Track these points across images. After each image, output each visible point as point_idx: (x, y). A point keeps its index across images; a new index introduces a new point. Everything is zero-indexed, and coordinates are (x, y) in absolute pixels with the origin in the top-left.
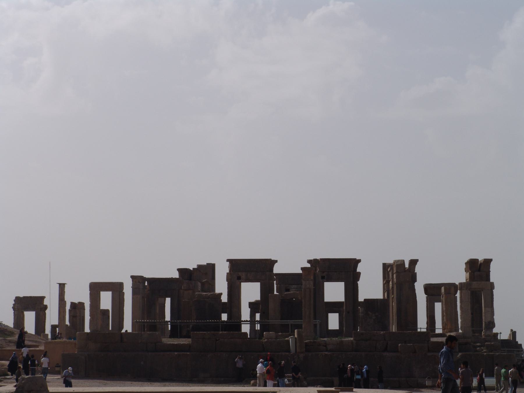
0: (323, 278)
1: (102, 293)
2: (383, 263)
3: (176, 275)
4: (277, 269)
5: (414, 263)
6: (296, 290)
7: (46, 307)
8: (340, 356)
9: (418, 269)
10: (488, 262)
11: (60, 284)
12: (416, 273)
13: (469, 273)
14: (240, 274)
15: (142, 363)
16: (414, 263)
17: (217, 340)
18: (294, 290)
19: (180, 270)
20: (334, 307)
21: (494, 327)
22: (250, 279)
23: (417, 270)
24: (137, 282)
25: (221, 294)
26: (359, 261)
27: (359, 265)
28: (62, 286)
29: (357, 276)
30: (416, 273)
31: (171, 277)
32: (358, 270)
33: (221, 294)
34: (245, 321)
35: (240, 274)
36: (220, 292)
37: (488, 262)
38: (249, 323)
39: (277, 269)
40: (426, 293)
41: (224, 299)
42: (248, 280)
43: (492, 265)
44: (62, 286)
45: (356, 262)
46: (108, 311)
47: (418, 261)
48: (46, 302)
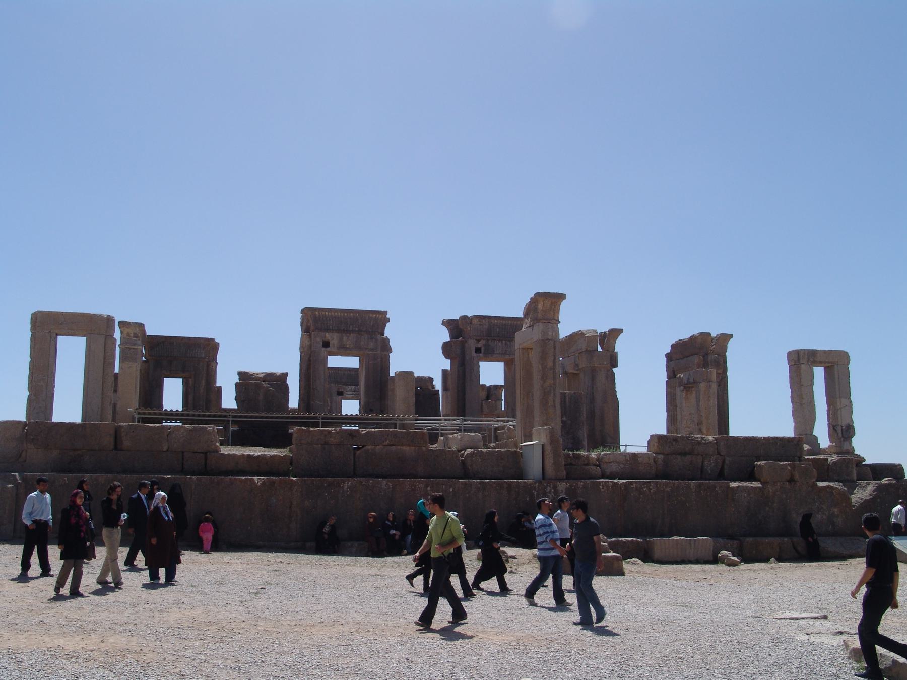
1: (63, 342)
2: (443, 370)
8: (645, 489)
12: (617, 352)
14: (328, 336)
18: (351, 393)
22: (348, 346)
24: (132, 335)
25: (285, 375)
30: (617, 352)
33: (285, 375)
35: (328, 336)
36: (284, 371)
37: (725, 338)
43: (731, 345)
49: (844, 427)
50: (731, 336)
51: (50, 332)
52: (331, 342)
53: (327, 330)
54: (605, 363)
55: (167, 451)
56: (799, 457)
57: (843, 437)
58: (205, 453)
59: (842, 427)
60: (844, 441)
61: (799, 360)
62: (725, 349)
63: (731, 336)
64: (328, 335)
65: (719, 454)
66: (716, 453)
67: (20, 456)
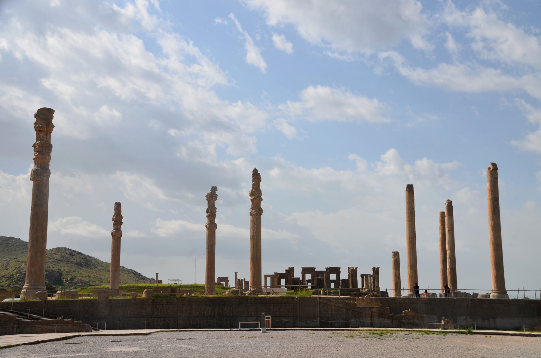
0: (330, 273)
3: (285, 272)
4: (316, 270)
5: (356, 268)
7: (228, 281)
9: (358, 270)
10: (378, 268)
11: (236, 273)
16: (356, 268)
19: (286, 270)
20: (333, 281)
25: (299, 278)
26: (340, 268)
27: (340, 269)
28: (236, 273)
29: (340, 272)
32: (340, 271)
33: (299, 278)
39: (316, 270)
40: (361, 277)
41: (301, 279)
42: (308, 274)
44: (236, 273)
45: (339, 268)
46: (248, 282)
48: (229, 279)
50: (379, 268)
53: (305, 271)
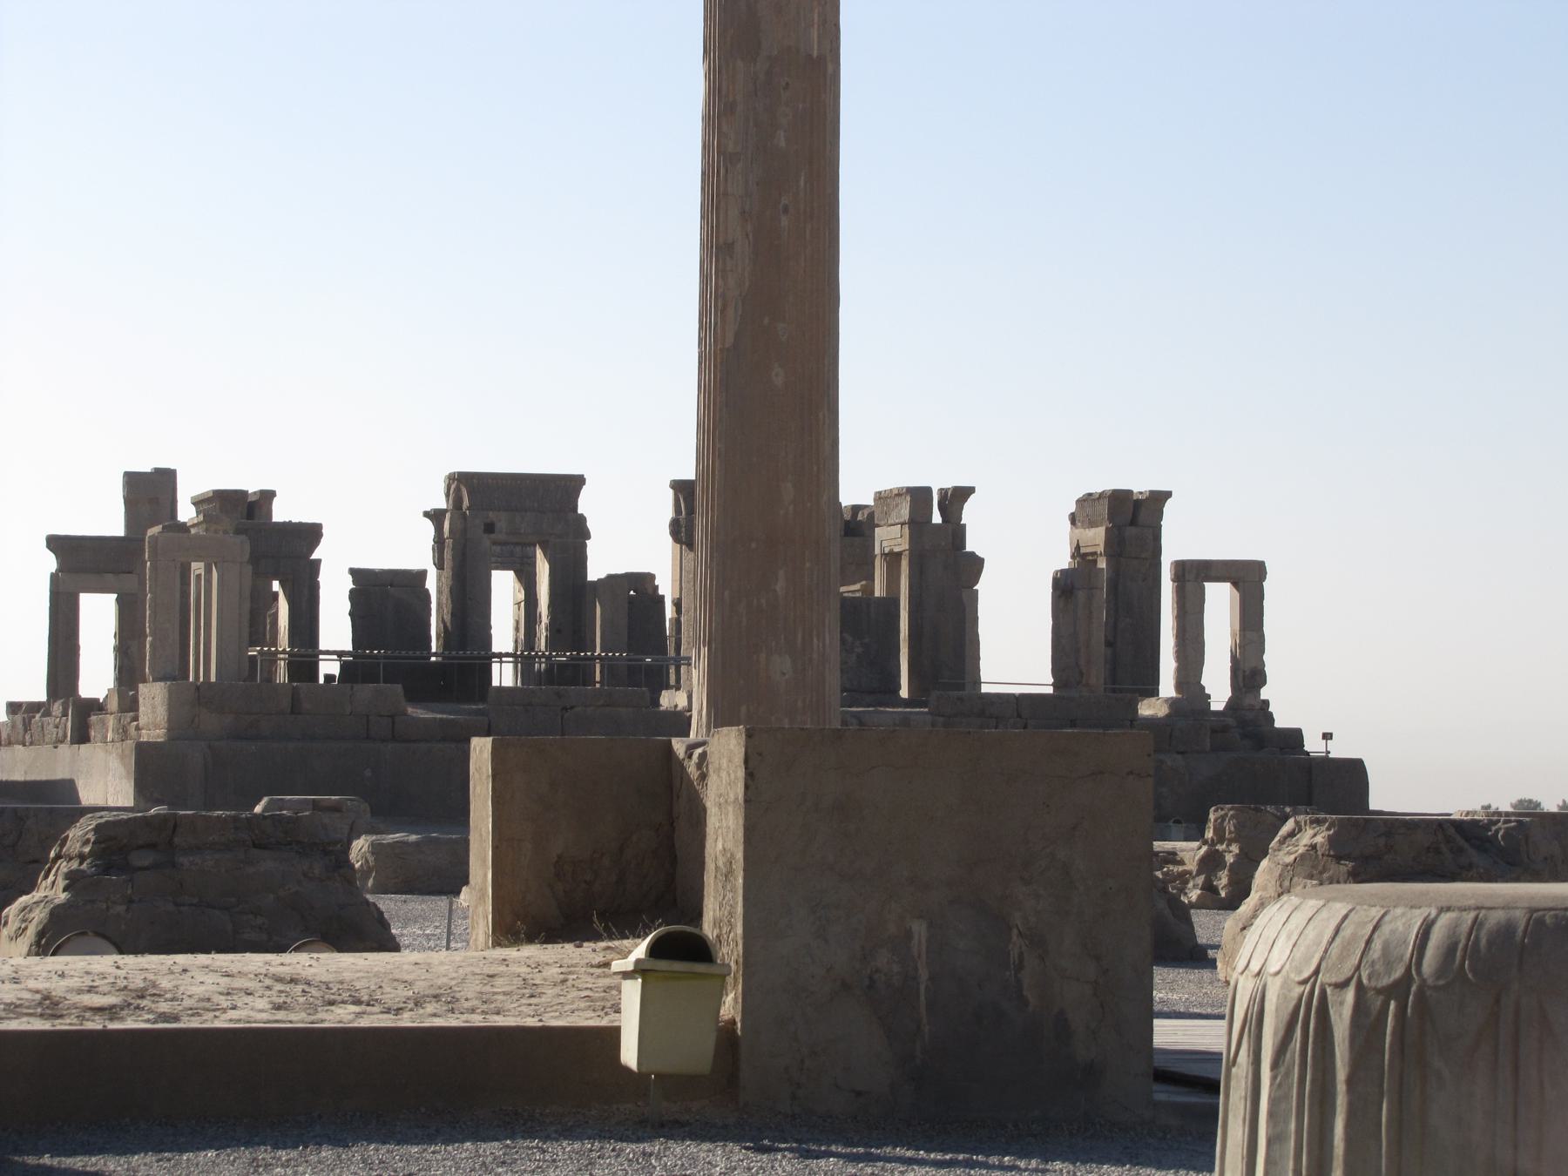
6: (499, 559)
9: (970, 514)
12: (965, 525)
13: (1107, 529)
15: (368, 773)
17: (565, 709)
21: (1264, 682)
22: (522, 531)
23: (966, 517)
30: (965, 525)
31: (287, 521)
34: (500, 655)
37: (1159, 499)
38: (511, 659)
43: (1169, 508)
47: (974, 492)
49: (1247, 673)
50: (1168, 495)
51: (174, 560)
52: (498, 526)
54: (943, 544)
55: (350, 714)
56: (1131, 721)
57: (1244, 686)
58: (392, 717)
59: (1244, 672)
60: (1246, 692)
61: (1184, 575)
62: (1159, 515)
63: (1168, 495)
64: (491, 514)
65: (1019, 716)
66: (1015, 714)
67: (193, 721)
